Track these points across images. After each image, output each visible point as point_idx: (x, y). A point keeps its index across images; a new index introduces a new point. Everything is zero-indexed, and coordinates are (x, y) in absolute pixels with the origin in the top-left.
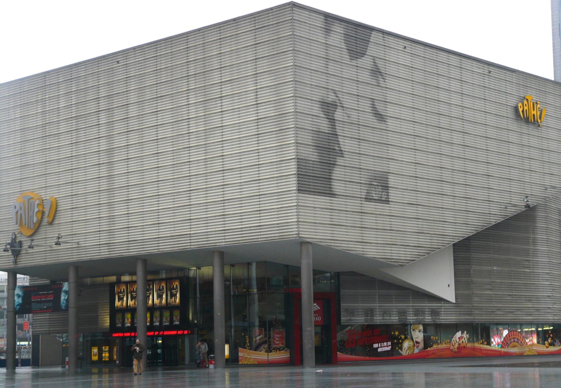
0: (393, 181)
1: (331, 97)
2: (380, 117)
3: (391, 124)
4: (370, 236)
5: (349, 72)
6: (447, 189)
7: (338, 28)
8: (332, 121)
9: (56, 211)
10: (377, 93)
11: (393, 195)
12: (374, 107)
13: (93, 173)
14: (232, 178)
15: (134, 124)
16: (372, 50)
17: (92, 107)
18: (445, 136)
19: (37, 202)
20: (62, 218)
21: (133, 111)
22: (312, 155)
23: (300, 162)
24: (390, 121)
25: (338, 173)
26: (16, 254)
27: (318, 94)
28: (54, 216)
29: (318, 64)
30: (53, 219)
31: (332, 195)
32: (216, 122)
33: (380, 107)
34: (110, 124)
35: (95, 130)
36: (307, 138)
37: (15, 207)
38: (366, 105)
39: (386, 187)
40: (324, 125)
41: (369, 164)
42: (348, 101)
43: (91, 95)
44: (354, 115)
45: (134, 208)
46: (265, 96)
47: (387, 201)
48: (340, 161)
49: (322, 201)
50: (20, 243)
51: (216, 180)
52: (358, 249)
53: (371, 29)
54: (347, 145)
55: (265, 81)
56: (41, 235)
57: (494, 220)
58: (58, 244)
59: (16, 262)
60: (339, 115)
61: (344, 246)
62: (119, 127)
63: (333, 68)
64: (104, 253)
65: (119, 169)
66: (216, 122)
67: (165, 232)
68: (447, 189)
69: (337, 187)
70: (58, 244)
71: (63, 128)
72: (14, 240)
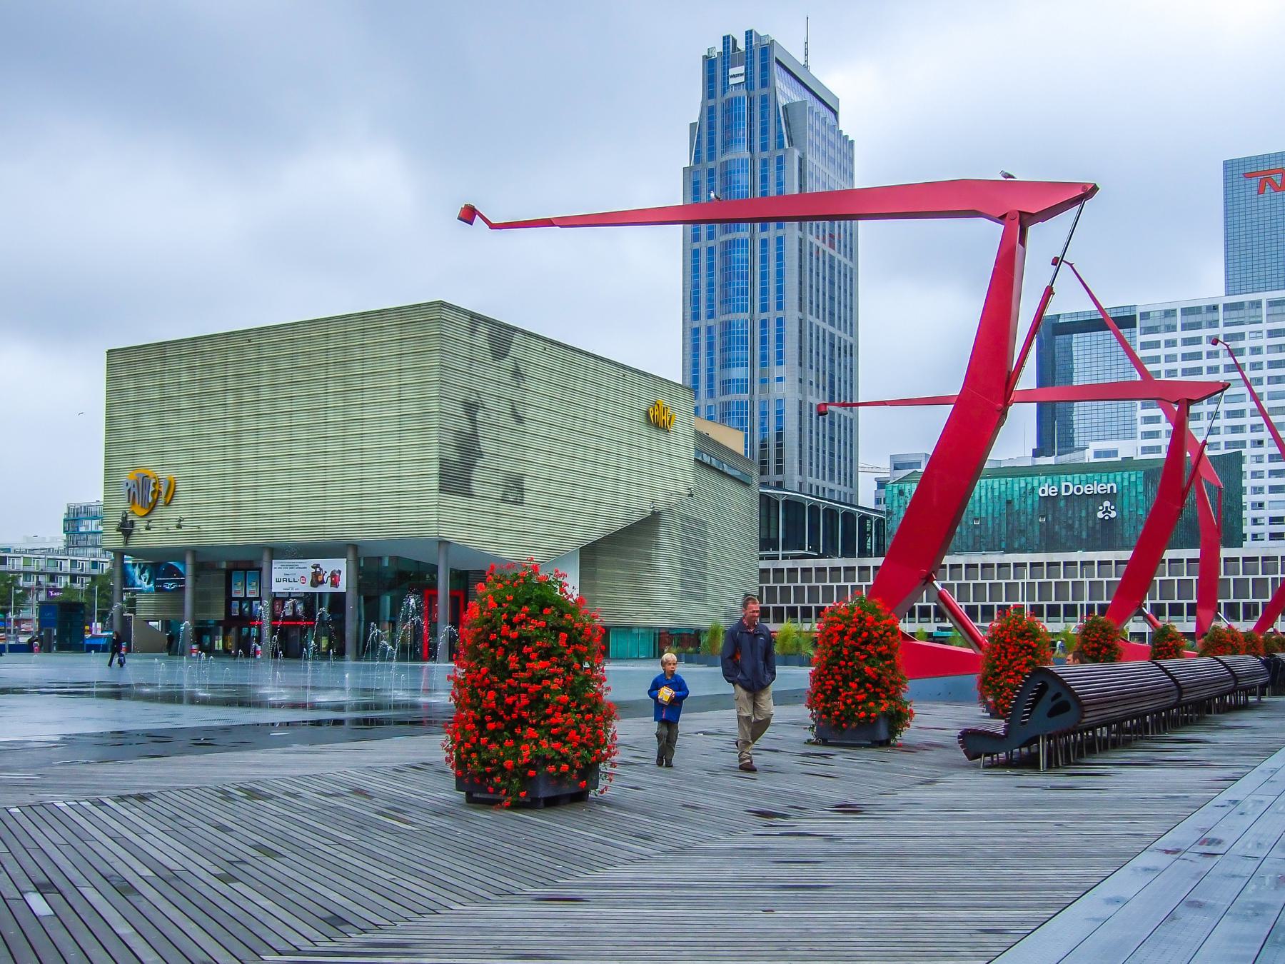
0: (528, 483)
1: (474, 398)
2: (519, 419)
3: (529, 426)
4: (504, 537)
5: (492, 374)
6: (578, 492)
7: (483, 329)
8: (473, 421)
9: (174, 491)
10: (515, 395)
11: (528, 497)
12: (513, 408)
13: (218, 454)
14: (371, 472)
15: (265, 409)
16: (514, 351)
17: (218, 385)
18: (579, 439)
19: (153, 481)
20: (181, 500)
21: (265, 394)
22: (453, 455)
23: (443, 462)
24: (528, 423)
25: (477, 474)
26: (127, 534)
27: (461, 395)
28: (172, 497)
29: (461, 365)
30: (171, 500)
31: (471, 496)
32: (355, 413)
33: (519, 408)
34: (239, 404)
35: (221, 409)
36: (450, 439)
37: (127, 484)
38: (505, 407)
39: (521, 490)
40: (466, 426)
41: (506, 466)
42: (490, 403)
43: (218, 373)
44: (494, 415)
45: (263, 494)
46: (409, 393)
47: (521, 503)
48: (479, 462)
49: (460, 501)
50: (132, 523)
51: (354, 473)
52: (491, 549)
53: (515, 329)
54: (487, 446)
55: (409, 378)
56: (155, 516)
57: (622, 524)
58: (179, 527)
59: (127, 542)
60: (480, 416)
61: (478, 546)
62: (248, 410)
63: (476, 369)
64: (229, 540)
65: (248, 453)
66: (355, 413)
67: (297, 522)
68: (578, 492)
69: (476, 488)
70: (179, 527)
71: (184, 404)
72: (125, 519)
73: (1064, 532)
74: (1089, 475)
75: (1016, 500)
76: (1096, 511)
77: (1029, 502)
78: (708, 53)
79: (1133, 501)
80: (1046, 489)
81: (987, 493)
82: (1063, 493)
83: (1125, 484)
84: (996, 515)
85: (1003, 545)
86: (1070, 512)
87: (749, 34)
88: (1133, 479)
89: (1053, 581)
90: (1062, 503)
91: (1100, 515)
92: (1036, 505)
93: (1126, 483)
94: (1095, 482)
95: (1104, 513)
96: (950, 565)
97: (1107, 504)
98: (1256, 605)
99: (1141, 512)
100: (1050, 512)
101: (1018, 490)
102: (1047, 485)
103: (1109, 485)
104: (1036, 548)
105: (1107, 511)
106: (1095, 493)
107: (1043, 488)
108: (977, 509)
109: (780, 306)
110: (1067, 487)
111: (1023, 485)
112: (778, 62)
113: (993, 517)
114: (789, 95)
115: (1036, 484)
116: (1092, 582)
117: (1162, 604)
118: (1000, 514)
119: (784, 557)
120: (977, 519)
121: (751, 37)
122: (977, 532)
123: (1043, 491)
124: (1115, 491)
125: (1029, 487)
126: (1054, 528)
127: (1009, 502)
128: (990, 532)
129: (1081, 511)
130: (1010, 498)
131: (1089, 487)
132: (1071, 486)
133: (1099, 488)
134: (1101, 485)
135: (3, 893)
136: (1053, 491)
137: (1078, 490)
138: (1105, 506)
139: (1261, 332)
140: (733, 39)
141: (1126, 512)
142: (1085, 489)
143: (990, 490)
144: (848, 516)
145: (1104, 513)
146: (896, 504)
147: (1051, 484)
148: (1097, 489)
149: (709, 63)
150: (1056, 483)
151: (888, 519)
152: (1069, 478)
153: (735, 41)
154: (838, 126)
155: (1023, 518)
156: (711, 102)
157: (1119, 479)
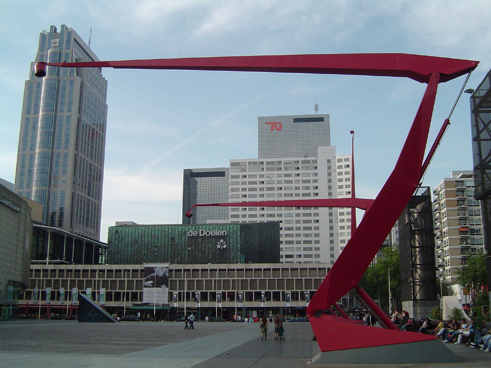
73: (200, 254)
74: (213, 226)
75: (176, 238)
76: (216, 244)
77: (183, 239)
78: (43, 32)
79: (235, 239)
80: (192, 232)
81: (161, 234)
82: (200, 235)
83: (230, 231)
84: (166, 245)
86: (204, 244)
87: (63, 26)
88: (235, 229)
89: (196, 279)
90: (200, 240)
91: (218, 246)
92: (187, 240)
93: (231, 231)
94: (216, 230)
95: (220, 245)
97: (222, 241)
98: (297, 293)
99: (239, 246)
100: (194, 244)
101: (177, 232)
102: (192, 231)
103: (223, 232)
104: (185, 262)
105: (221, 245)
106: (216, 235)
108: (156, 241)
109: (66, 147)
110: (202, 232)
111: (180, 230)
112: (75, 40)
113: (164, 246)
114: (79, 55)
115: (187, 229)
117: (278, 292)
118: (168, 245)
121: (64, 28)
122: (156, 254)
123: (190, 234)
124: (226, 235)
125: (183, 231)
126: (195, 253)
127: (172, 239)
128: (163, 253)
129: (209, 245)
130: (173, 236)
131: (213, 232)
132: (204, 232)
133: (218, 233)
134: (219, 231)
136: (195, 233)
137: (208, 233)
138: (221, 242)
139: (281, 174)
140: (55, 28)
141: (231, 246)
142: (211, 233)
144: (89, 245)
145: (220, 245)
146: (114, 238)
147: (194, 230)
148: (217, 233)
149: (43, 36)
150: (196, 230)
151: (109, 245)
152: (204, 227)
153: (56, 29)
154: (101, 73)
155: (180, 247)
156: (42, 53)
157: (228, 228)
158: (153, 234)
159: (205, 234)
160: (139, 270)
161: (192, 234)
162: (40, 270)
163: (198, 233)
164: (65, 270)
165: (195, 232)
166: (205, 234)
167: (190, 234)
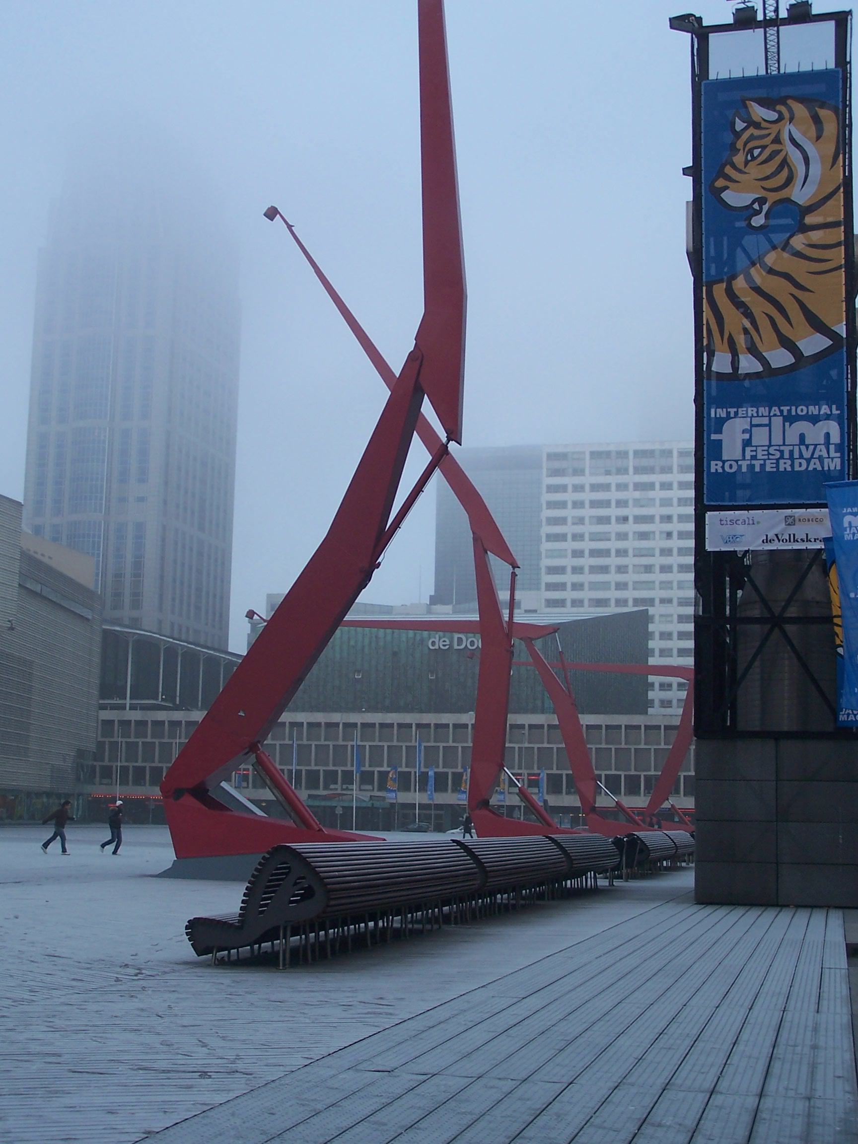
80: (437, 641)
82: (456, 647)
85: (387, 702)
89: (441, 745)
96: (435, 724)
107: (433, 640)
116: (617, 748)
119: (133, 708)
120: (359, 672)
123: (433, 643)
127: (395, 654)
135: (387, 1141)
136: (445, 643)
143: (374, 639)
158: (352, 643)
159: (466, 645)
160: (323, 724)
161: (437, 643)
162: (114, 721)
163: (451, 641)
164: (166, 723)
165: (444, 641)
166: (466, 645)
167: (433, 643)
